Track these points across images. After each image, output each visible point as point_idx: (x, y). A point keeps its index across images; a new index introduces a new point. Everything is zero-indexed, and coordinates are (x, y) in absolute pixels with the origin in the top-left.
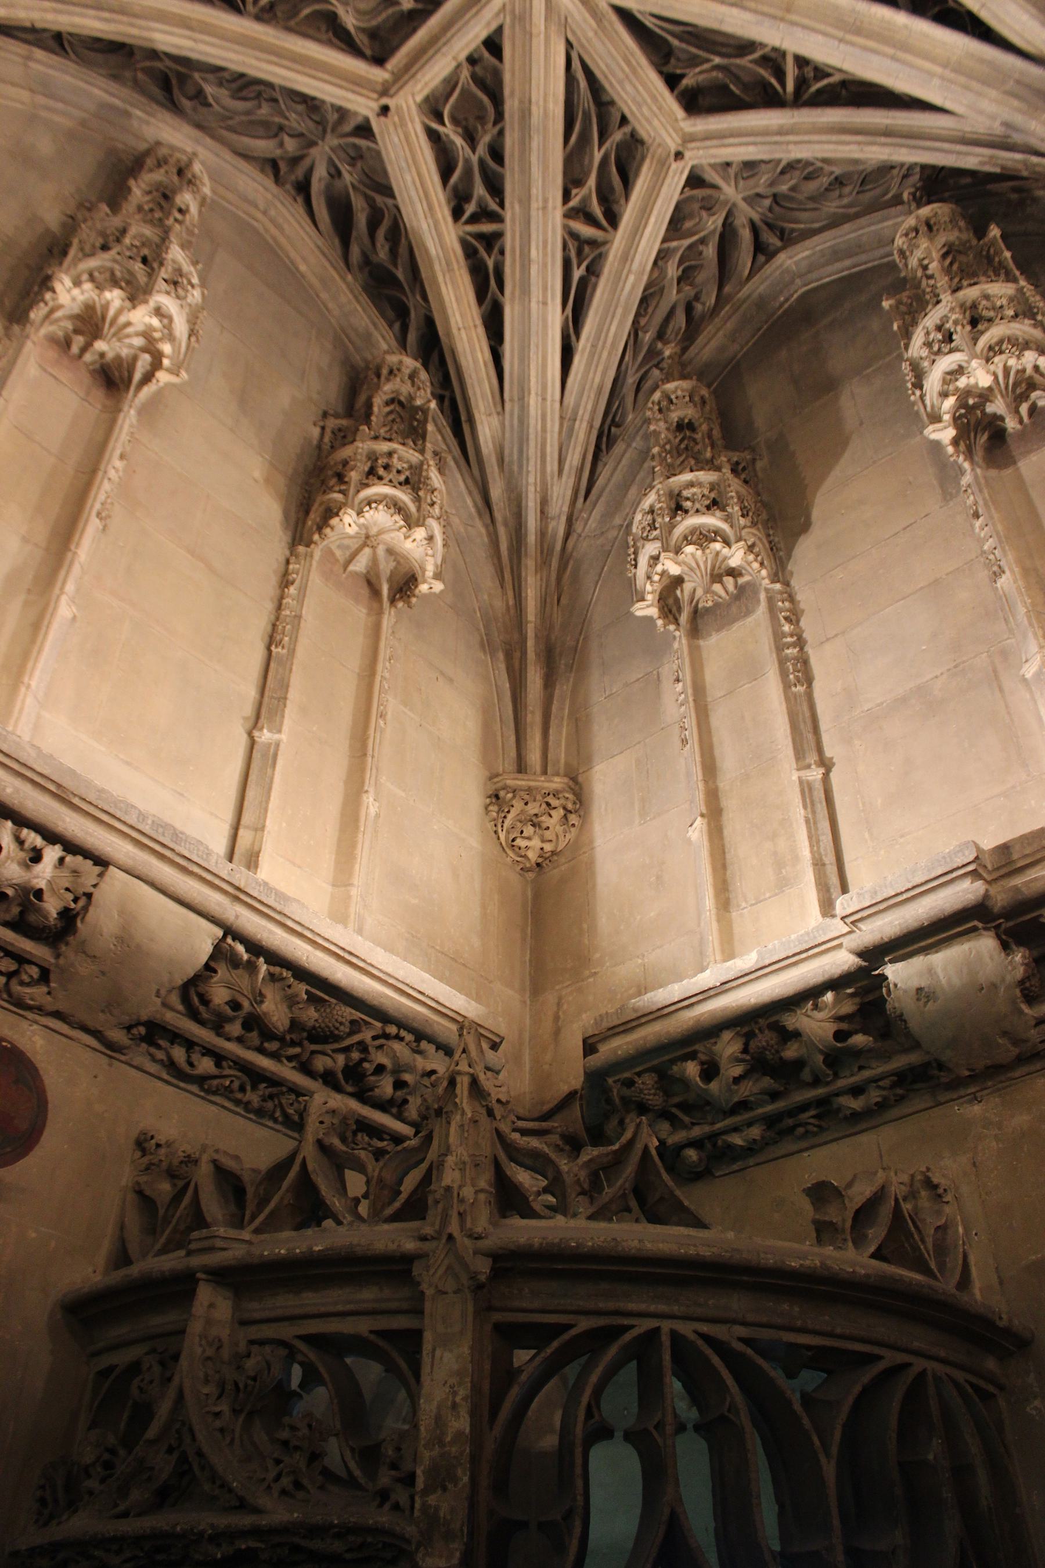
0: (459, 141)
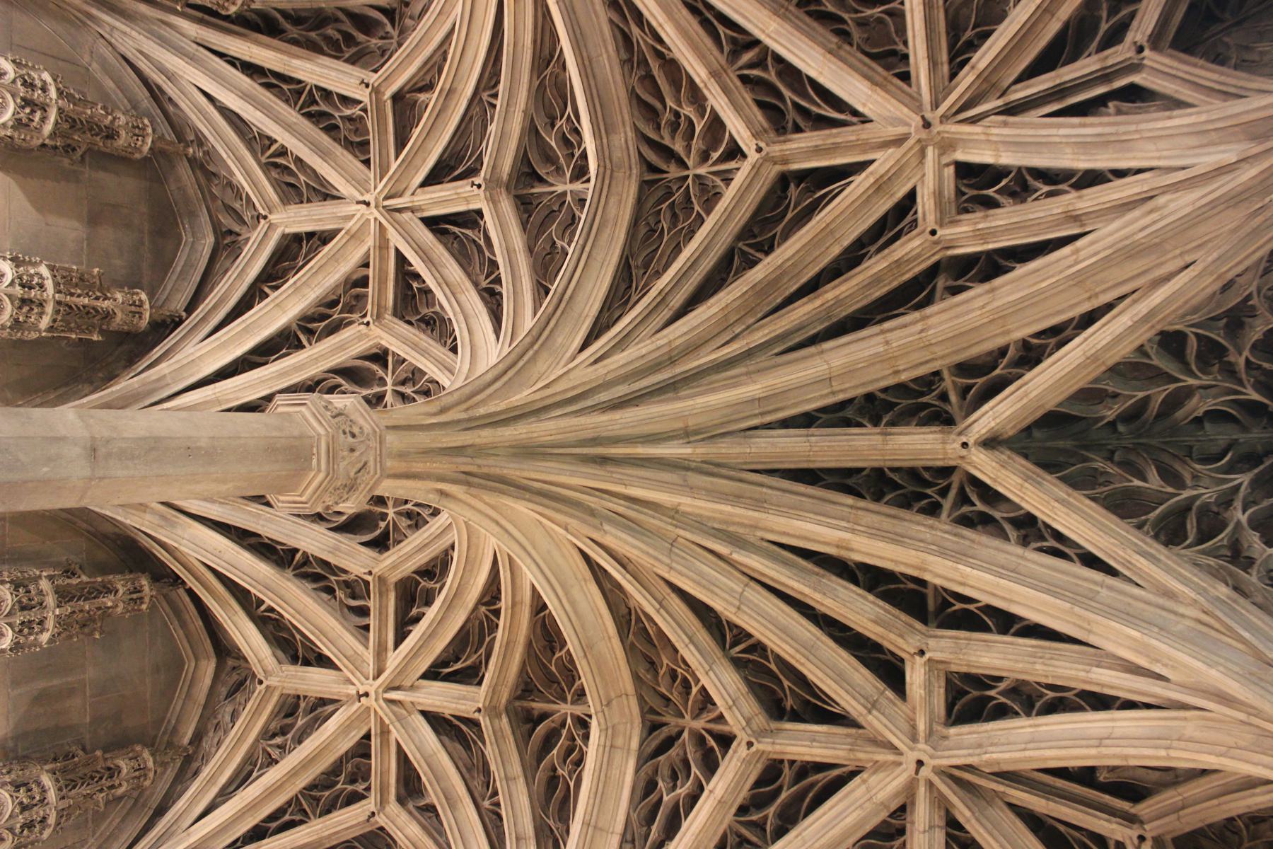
0: (348, 112)
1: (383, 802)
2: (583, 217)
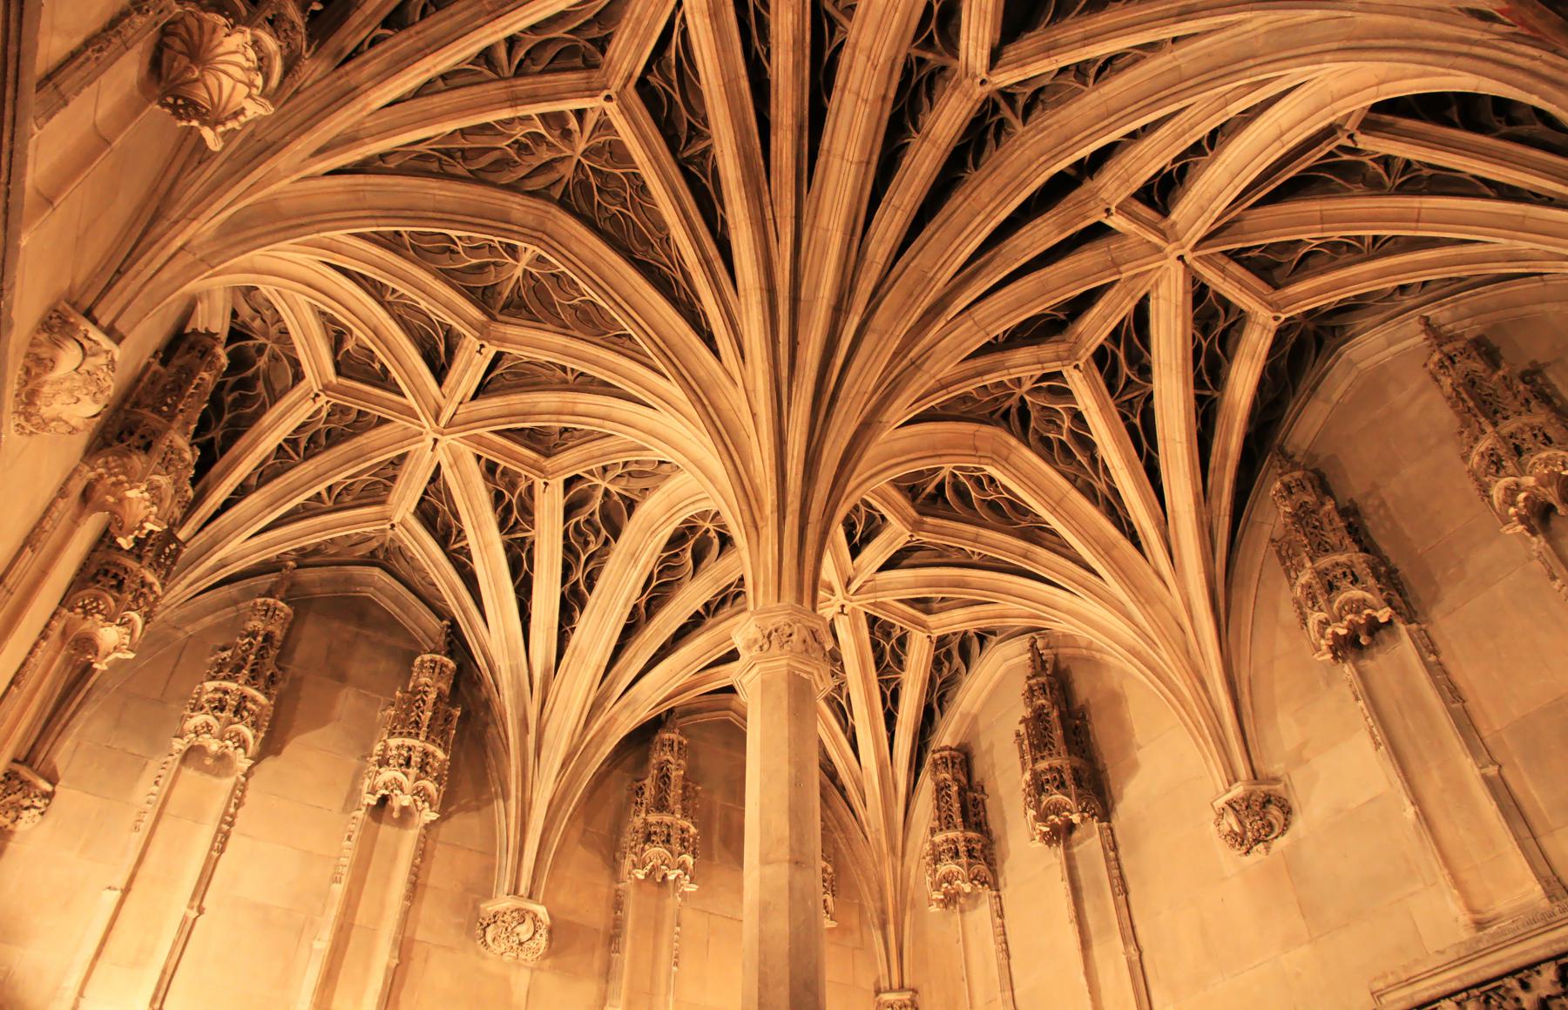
0: (324, 414)
1: (923, 626)
2: (562, 268)
